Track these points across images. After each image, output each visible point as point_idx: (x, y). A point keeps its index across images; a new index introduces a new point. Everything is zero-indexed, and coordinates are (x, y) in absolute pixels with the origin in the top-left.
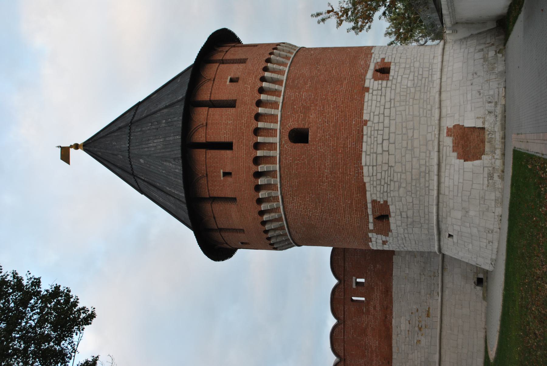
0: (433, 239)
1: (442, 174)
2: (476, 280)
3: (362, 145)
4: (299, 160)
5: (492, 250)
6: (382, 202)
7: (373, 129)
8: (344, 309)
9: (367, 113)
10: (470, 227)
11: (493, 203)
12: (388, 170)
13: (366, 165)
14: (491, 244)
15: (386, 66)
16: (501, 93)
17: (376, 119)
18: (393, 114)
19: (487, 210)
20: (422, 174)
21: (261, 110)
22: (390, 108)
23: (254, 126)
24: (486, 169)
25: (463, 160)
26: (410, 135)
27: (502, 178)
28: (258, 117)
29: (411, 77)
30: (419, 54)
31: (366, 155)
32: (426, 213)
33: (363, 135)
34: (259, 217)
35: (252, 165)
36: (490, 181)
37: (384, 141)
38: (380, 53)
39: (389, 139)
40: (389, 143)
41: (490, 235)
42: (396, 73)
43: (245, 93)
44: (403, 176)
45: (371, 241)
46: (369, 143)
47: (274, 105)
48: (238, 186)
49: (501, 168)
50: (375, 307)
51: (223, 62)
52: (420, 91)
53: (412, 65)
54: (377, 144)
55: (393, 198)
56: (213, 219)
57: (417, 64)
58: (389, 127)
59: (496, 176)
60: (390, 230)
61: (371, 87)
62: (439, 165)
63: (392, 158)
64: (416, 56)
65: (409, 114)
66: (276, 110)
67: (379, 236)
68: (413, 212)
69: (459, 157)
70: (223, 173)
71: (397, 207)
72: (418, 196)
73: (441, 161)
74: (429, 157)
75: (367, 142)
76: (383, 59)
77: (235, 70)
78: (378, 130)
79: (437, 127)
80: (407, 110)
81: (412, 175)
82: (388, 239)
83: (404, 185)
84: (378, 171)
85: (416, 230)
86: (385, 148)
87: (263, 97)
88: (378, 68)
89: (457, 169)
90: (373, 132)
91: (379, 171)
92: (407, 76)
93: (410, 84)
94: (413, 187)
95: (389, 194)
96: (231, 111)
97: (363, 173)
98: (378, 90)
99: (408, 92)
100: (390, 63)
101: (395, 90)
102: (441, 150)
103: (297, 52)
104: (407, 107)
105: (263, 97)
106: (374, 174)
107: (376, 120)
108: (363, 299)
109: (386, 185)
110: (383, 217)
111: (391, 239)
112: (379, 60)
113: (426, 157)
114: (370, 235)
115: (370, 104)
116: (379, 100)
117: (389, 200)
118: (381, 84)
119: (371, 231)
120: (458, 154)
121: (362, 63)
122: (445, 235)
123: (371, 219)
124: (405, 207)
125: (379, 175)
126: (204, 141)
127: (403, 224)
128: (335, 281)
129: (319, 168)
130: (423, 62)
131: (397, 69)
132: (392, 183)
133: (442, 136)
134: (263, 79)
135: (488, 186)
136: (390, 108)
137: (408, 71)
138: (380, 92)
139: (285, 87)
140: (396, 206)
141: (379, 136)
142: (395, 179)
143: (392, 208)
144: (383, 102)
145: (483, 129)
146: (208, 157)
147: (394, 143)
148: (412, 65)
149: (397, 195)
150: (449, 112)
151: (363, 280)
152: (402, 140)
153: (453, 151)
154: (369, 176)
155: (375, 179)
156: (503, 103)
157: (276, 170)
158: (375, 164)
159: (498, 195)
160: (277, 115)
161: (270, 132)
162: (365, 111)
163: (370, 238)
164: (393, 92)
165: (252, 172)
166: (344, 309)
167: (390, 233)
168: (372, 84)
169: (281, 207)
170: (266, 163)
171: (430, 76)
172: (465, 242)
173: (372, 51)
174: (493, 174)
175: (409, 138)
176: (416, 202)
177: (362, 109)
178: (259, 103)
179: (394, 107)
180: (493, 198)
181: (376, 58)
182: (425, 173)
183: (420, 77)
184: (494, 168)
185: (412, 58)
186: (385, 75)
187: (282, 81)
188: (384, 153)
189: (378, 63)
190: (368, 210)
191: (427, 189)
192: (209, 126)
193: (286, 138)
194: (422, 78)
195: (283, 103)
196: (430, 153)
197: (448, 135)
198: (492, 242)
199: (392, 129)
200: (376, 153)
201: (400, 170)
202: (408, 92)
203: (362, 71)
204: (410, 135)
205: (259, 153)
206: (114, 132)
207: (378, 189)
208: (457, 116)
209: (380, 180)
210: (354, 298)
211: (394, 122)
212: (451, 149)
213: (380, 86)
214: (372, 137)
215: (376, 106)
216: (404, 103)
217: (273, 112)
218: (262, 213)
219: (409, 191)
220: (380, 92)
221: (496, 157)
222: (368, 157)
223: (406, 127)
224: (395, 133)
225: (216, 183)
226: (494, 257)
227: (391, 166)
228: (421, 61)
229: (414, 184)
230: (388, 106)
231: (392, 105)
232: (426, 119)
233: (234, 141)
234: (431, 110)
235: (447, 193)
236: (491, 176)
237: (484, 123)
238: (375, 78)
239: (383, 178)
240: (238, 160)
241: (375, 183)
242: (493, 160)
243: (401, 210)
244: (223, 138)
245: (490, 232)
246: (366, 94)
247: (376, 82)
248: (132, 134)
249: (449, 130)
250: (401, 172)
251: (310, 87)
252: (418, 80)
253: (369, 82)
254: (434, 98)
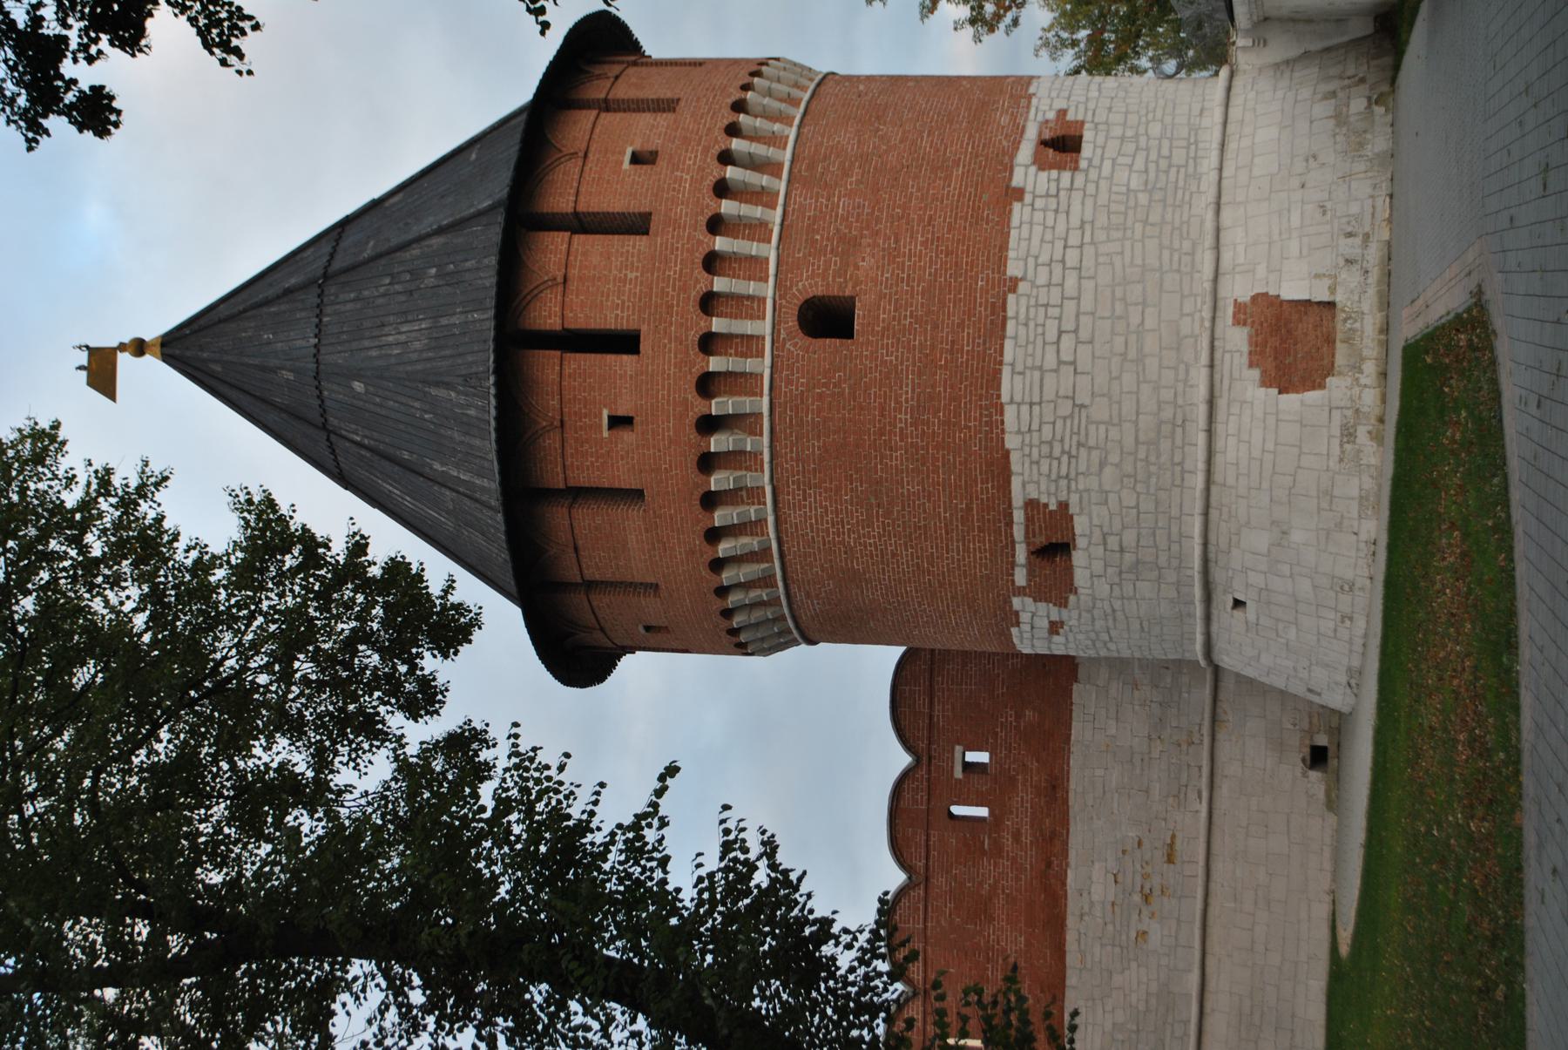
0: (1191, 615)
1: (1220, 428)
2: (1307, 751)
3: (1002, 346)
4: (825, 385)
5: (1351, 642)
6: (1053, 507)
7: (1032, 302)
8: (927, 840)
9: (1017, 259)
10: (1291, 576)
11: (1355, 506)
12: (1072, 416)
13: (1012, 402)
14: (1348, 623)
15: (1072, 132)
16: (1379, 209)
17: (1043, 271)
18: (1089, 262)
19: (1339, 525)
20: (1166, 429)
21: (720, 243)
22: (1081, 246)
23: (702, 288)
24: (1336, 415)
25: (1275, 391)
26: (1135, 320)
27: (1378, 438)
28: (712, 262)
29: (1139, 164)
30: (1161, 102)
31: (1013, 372)
32: (1175, 537)
33: (1005, 319)
34: (706, 547)
35: (692, 395)
36: (1348, 447)
37: (1064, 336)
38: (1054, 94)
39: (1076, 331)
40: (1078, 342)
41: (1345, 599)
42: (1099, 151)
43: (677, 192)
44: (1114, 433)
45: (1018, 624)
46: (1022, 340)
47: (758, 230)
48: (652, 456)
49: (1377, 411)
50: (1017, 836)
51: (607, 106)
52: (1164, 200)
53: (1142, 130)
54: (1045, 343)
55: (1085, 495)
56: (571, 550)
57: (1155, 129)
58: (1079, 299)
59: (1362, 432)
60: (1073, 589)
61: (1029, 188)
62: (1211, 403)
63: (1083, 381)
64: (1152, 105)
65: (1132, 264)
66: (763, 246)
67: (1042, 606)
68: (1139, 534)
69: (1266, 382)
70: (611, 418)
71: (1096, 521)
72: (1152, 491)
73: (1217, 393)
74: (1186, 381)
75: (1015, 338)
76: (1062, 113)
77: (644, 130)
78: (1046, 306)
79: (1209, 299)
80: (1128, 254)
81: (1137, 431)
82: (1065, 613)
83: (1114, 458)
84: (1046, 419)
85: (1145, 588)
86: (1066, 356)
87: (727, 207)
88: (1047, 135)
89: (1259, 414)
90: (1032, 310)
91: (1049, 418)
92: (1128, 160)
93: (1135, 183)
94: (1139, 464)
95: (1073, 484)
96: (635, 244)
97: (1003, 422)
98: (1048, 195)
99: (1132, 203)
100: (1083, 123)
101: (1095, 196)
102: (1217, 362)
103: (819, 85)
104: (1128, 244)
105: (727, 207)
106: (1035, 426)
107: (1042, 279)
108: (983, 812)
109: (1065, 459)
110: (1054, 550)
111: (1075, 614)
112: (1051, 115)
113: (1177, 380)
114: (1016, 602)
115: (1025, 234)
116: (1050, 222)
117: (1074, 500)
118: (1058, 180)
119: (1021, 592)
120: (1264, 373)
121: (1004, 120)
122: (1223, 601)
123: (1021, 554)
125: (1047, 429)
126: (558, 328)
127: (1110, 570)
128: (904, 759)
129: (882, 409)
130: (1173, 124)
131: (1100, 140)
132: (1083, 452)
133: (1219, 322)
134: (726, 158)
135: (1341, 460)
136: (1081, 246)
137: (1130, 148)
138: (1054, 200)
139: (789, 181)
140: (1091, 519)
141: (1049, 322)
142: (1092, 443)
143: (1080, 524)
144: (1061, 228)
145: (1331, 305)
146: (567, 371)
147: (1091, 342)
148: (1142, 130)
149: (1095, 486)
150: (1241, 260)
151: (982, 757)
152: (1113, 333)
153: (1251, 365)
154: (1019, 432)
155: (1036, 441)
156: (1386, 236)
157: (761, 414)
158: (1036, 399)
159: (1368, 483)
160: (767, 259)
161: (745, 306)
162: (1011, 254)
163: (1017, 613)
164: (1089, 202)
165: (692, 417)
166: (927, 840)
167: (1072, 598)
168: (1031, 179)
169: (771, 519)
170: (732, 393)
171: (1191, 162)
172: (1278, 620)
173: (1032, 90)
174: (1354, 426)
175: (1132, 328)
176: (1147, 505)
177: (1004, 247)
178: (716, 225)
179: (1092, 243)
180: (1355, 493)
181: (1043, 108)
182: (1174, 425)
183: (1163, 164)
184: (1357, 411)
185: (1143, 112)
186: (1067, 157)
187: (780, 165)
188: (1064, 368)
189: (1047, 121)
190: (1015, 527)
191: (1178, 469)
192: (573, 286)
193: (793, 323)
194: (1170, 166)
195: (782, 224)
196: (1187, 371)
197: (1238, 321)
198: (1351, 619)
199: (1087, 305)
200: (1040, 368)
201: (1106, 418)
202: (1132, 203)
203: (1005, 143)
204: (1135, 320)
205: (715, 364)
206: (267, 302)
207: (1045, 468)
208: (1261, 271)
209: (1050, 443)
210: (957, 810)
211: (1091, 284)
212: (1245, 360)
213: (1053, 185)
214: (1032, 324)
215: (1042, 241)
216: (1119, 234)
217: (754, 248)
218: (714, 535)
219: (1129, 476)
220: (1053, 203)
221: (1363, 381)
222: (1018, 378)
223: (1124, 299)
224: (1092, 314)
225: (586, 446)
226: (1356, 663)
227: (1082, 406)
228: (1168, 119)
229: (1142, 455)
230: (1074, 239)
231: (1087, 239)
232: (1177, 277)
233: (644, 328)
234: (1193, 254)
235: (1231, 481)
236: (1348, 434)
237: (1332, 290)
238: (1041, 163)
239: (1058, 437)
240: (652, 383)
241: (1035, 451)
242: (1356, 390)
243: (1106, 530)
244: (612, 319)
245: (1346, 588)
246: (1017, 206)
247: (1043, 175)
248: (328, 310)
249: (1239, 307)
250: (1109, 423)
251: (859, 182)
252: (1158, 170)
253: (1024, 173)
254: (1202, 223)
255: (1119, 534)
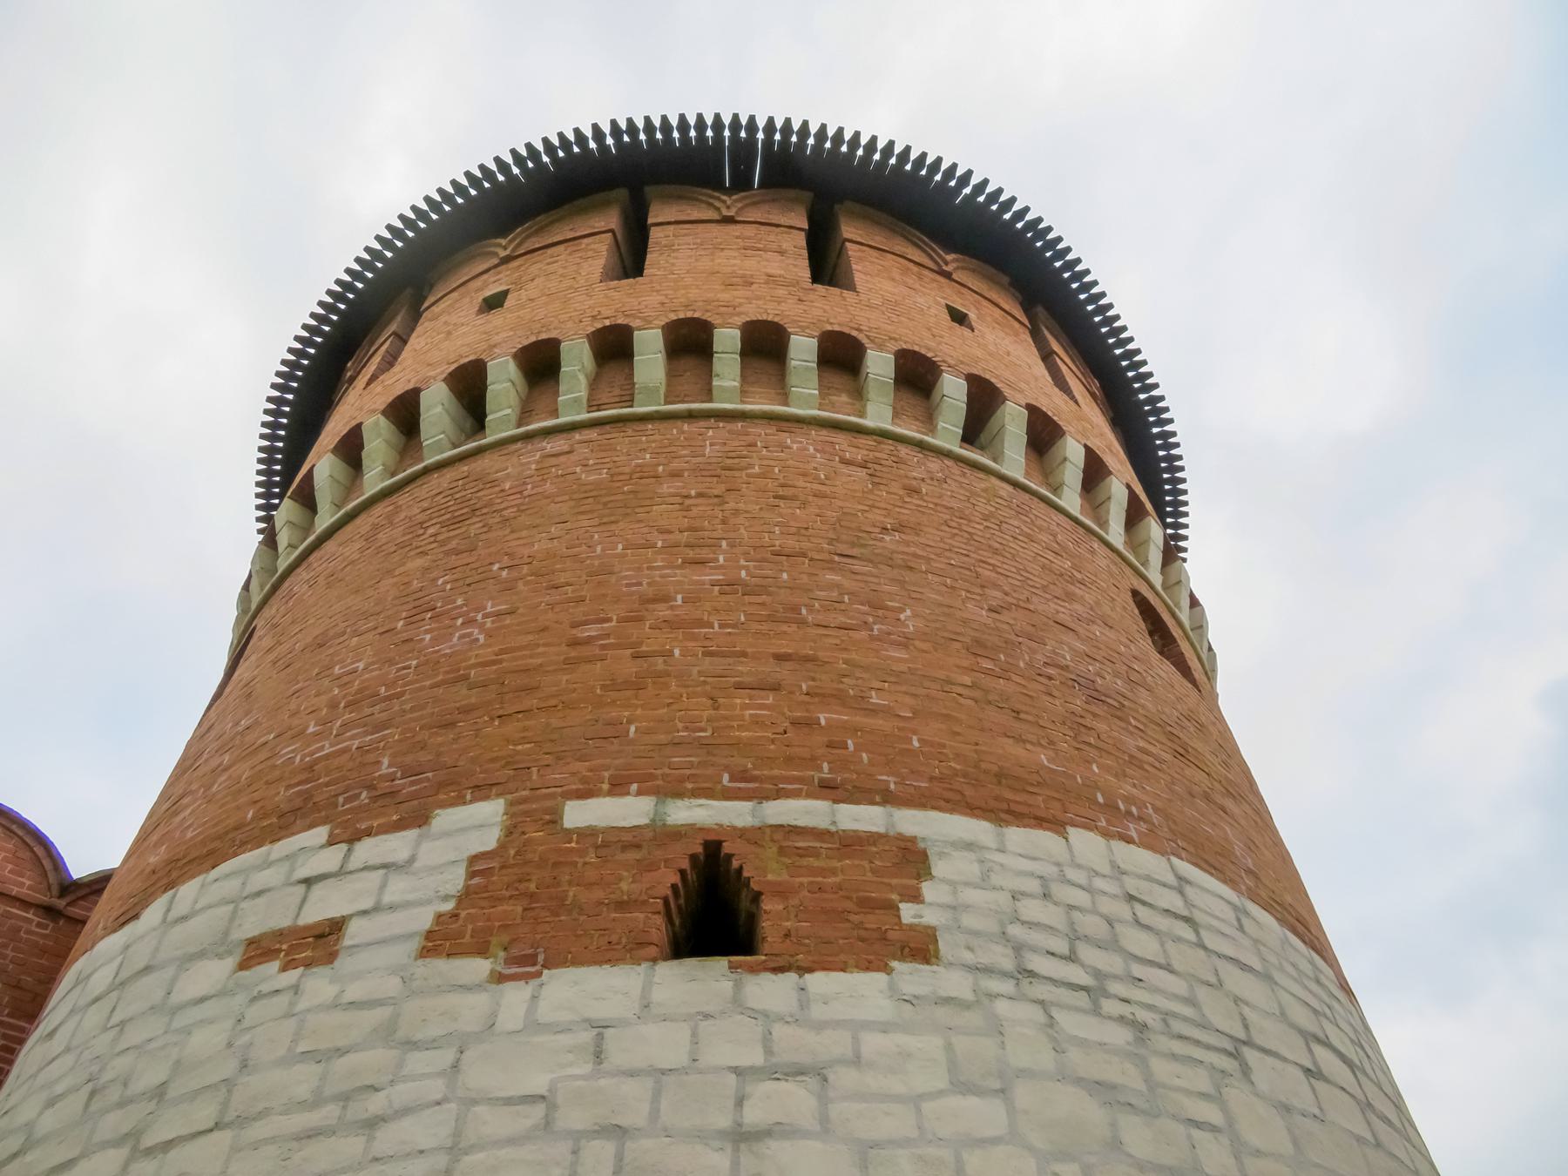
55: (973, 1018)
60: (526, 962)
71: (872, 1043)
110: (714, 915)
117: (948, 980)
123: (689, 813)
124: (893, 1123)
140: (885, 1028)
190: (821, 806)
207: (1033, 909)
243: (844, 1078)
255: (825, 1127)
